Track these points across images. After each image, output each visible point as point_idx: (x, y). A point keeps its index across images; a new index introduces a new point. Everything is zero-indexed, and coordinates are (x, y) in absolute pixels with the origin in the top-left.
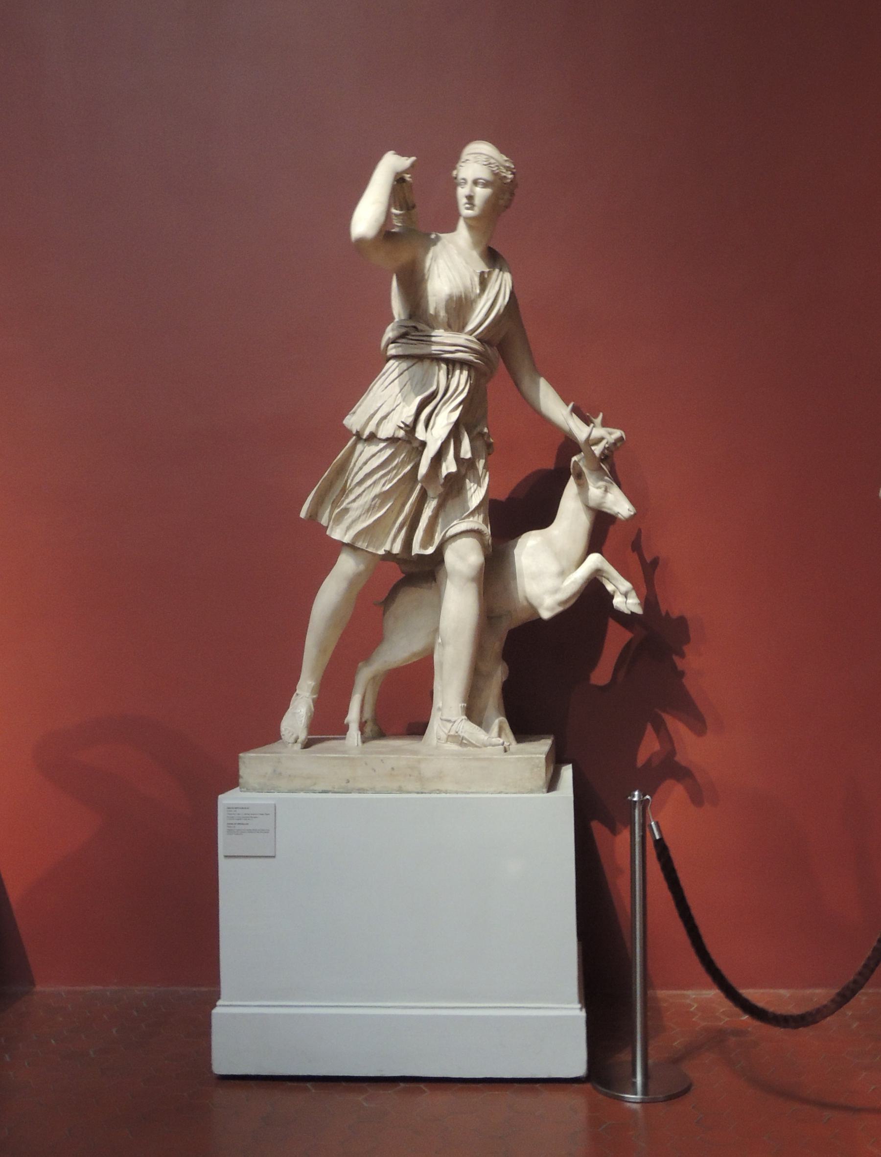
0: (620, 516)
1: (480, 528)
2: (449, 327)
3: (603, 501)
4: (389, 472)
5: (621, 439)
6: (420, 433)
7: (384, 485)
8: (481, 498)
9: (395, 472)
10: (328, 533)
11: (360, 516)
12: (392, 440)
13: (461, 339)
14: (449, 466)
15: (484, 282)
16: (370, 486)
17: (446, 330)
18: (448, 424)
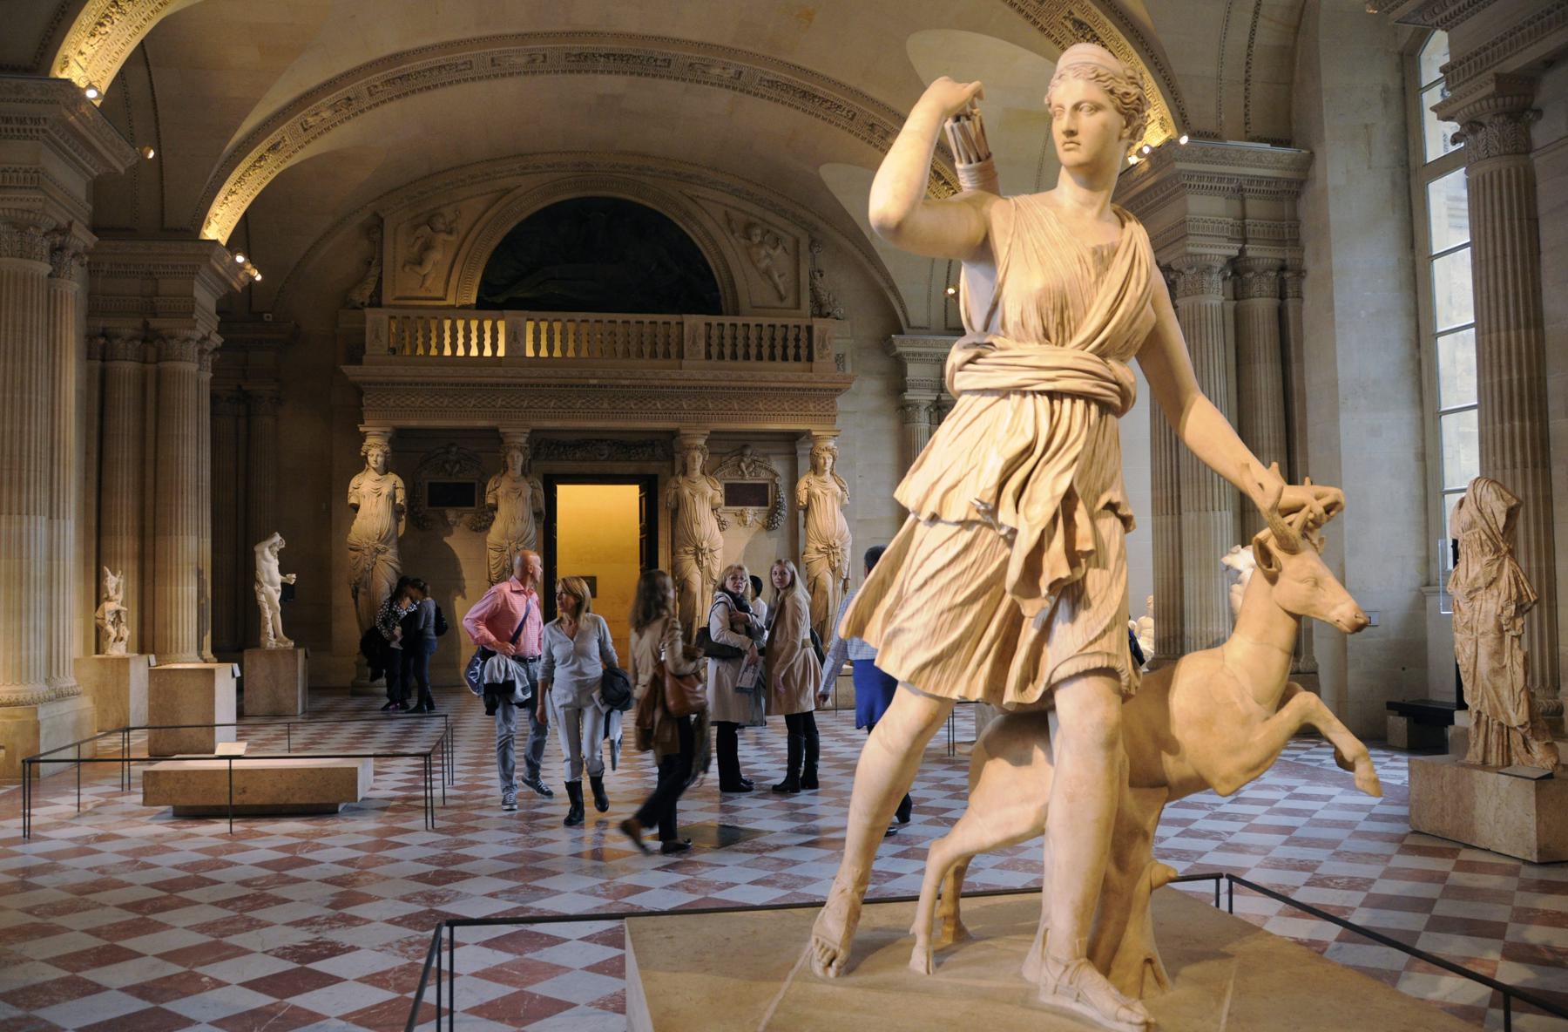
6: (1006, 515)
7: (955, 593)
10: (876, 664)
12: (965, 524)
13: (1070, 355)
15: (1103, 259)
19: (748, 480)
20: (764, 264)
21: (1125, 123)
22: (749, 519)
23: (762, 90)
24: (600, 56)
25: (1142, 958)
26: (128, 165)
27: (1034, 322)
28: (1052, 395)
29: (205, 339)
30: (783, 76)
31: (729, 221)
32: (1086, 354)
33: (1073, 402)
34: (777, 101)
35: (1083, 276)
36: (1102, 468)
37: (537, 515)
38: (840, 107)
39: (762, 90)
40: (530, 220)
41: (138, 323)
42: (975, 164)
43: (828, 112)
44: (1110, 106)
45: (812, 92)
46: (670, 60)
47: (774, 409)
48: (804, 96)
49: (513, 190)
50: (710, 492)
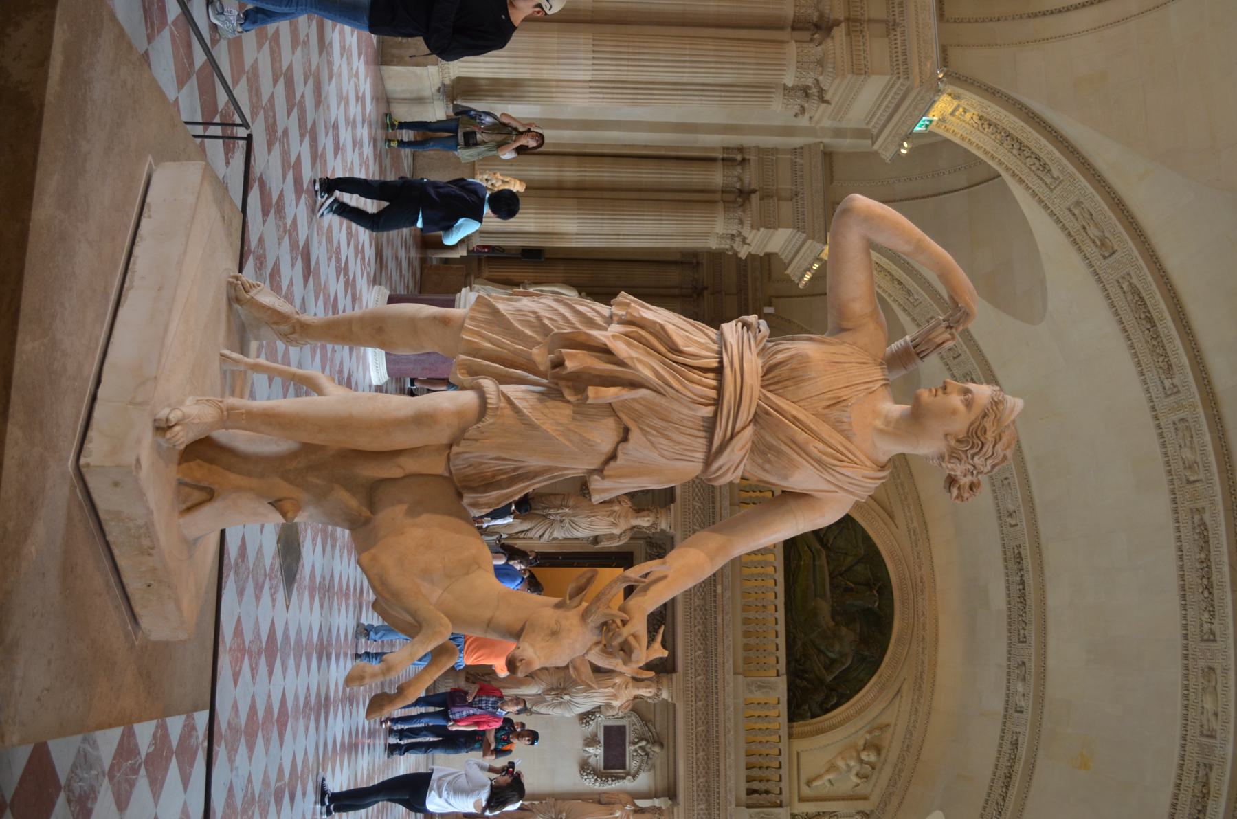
7: (551, 319)
19: (630, 749)
20: (841, 763)
21: (961, 437)
22: (591, 750)
23: (1008, 737)
24: (1022, 576)
25: (216, 487)
26: (880, 151)
27: (780, 357)
28: (719, 371)
29: (744, 240)
30: (1023, 753)
31: (883, 728)
33: (714, 388)
34: (999, 752)
35: (823, 400)
36: (657, 432)
37: (596, 540)
38: (1000, 813)
39: (1008, 737)
40: (867, 539)
41: (753, 187)
42: (910, 344)
43: (994, 804)
44: (972, 417)
45: (1012, 783)
46: (1025, 642)
47: (698, 767)
48: (1006, 777)
49: (893, 521)
50: (616, 703)
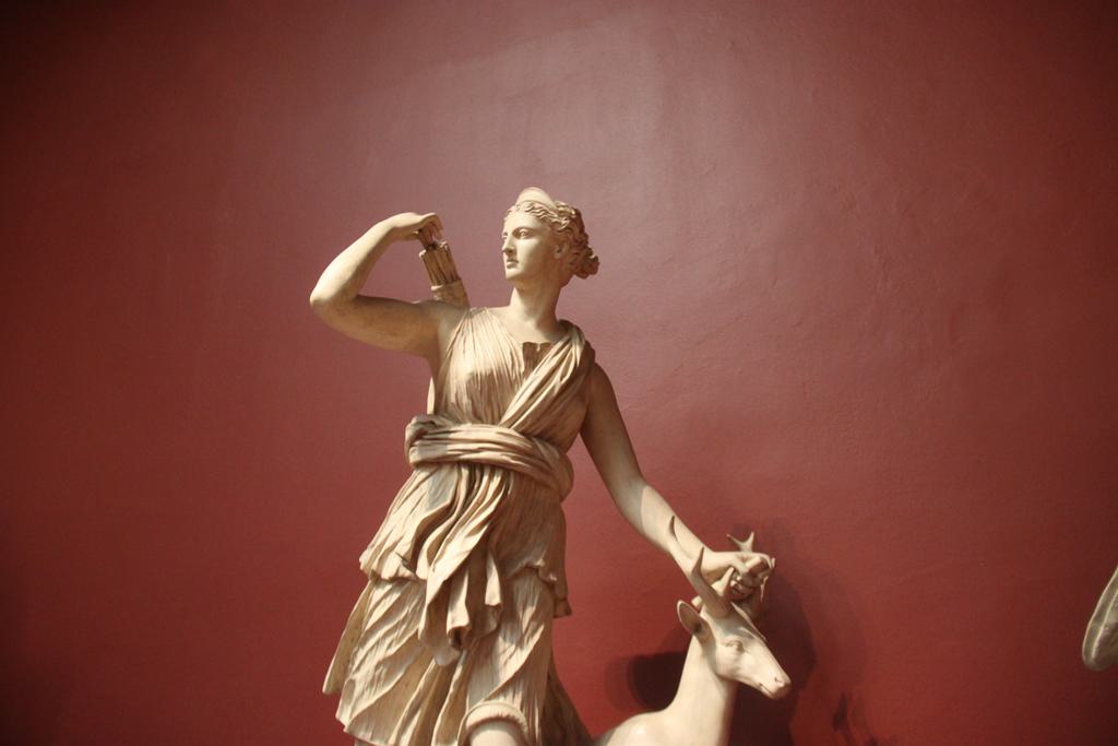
0: (764, 690)
1: (512, 715)
2: (477, 418)
3: (737, 665)
4: (395, 628)
5: (763, 566)
6: (423, 569)
7: (389, 646)
8: (523, 661)
9: (404, 627)
10: (337, 715)
11: (363, 693)
12: (397, 580)
13: (490, 432)
14: (458, 616)
16: (373, 647)
17: (473, 422)
18: (458, 555)
28: (471, 465)
32: (511, 431)
